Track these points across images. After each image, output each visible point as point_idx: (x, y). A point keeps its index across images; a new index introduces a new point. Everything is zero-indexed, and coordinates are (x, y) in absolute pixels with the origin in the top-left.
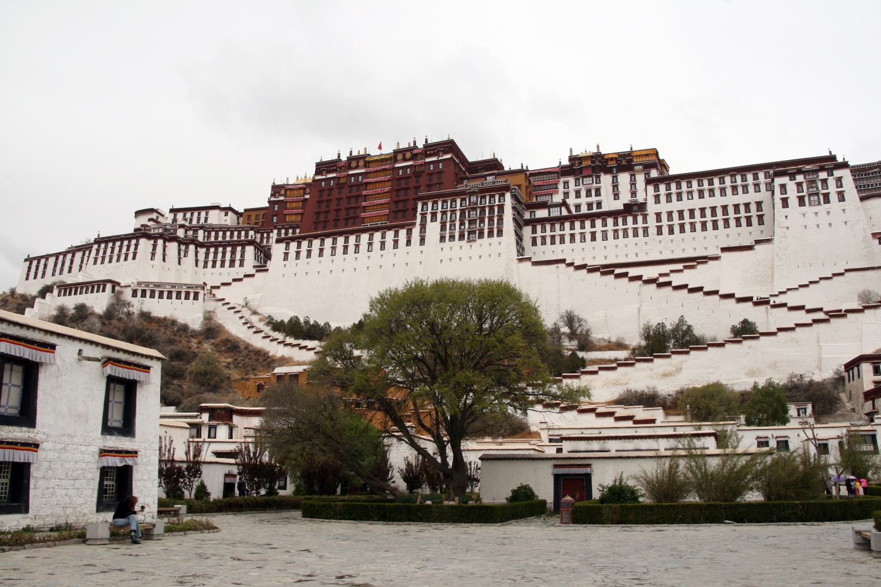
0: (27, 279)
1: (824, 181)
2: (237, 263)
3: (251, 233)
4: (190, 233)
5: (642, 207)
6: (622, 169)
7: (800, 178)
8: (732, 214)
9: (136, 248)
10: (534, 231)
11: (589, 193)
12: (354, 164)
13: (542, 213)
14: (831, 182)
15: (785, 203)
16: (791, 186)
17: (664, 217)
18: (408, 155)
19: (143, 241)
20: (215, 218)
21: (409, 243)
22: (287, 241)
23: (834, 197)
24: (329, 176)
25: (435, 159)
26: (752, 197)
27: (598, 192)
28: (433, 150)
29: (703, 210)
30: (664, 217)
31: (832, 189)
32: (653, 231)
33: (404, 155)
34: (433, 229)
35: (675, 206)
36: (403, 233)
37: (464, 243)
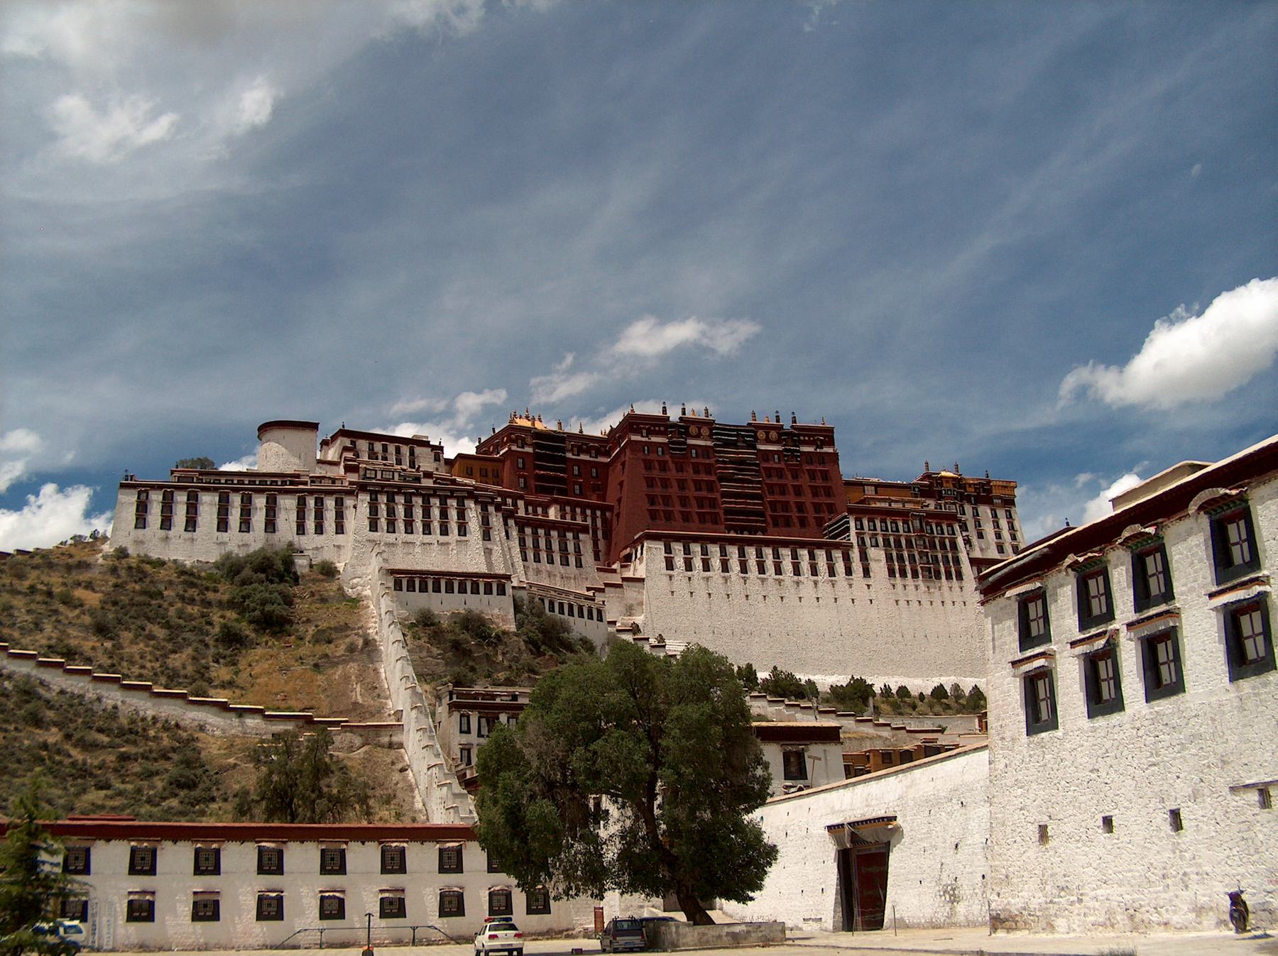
0: (141, 522)
2: (572, 560)
3: (521, 503)
9: (461, 514)
12: (693, 430)
18: (773, 435)
19: (470, 504)
20: (426, 463)
21: (849, 571)
22: (667, 540)
24: (654, 439)
25: (811, 449)
28: (809, 436)
33: (767, 434)
34: (877, 556)
36: (837, 554)
37: (920, 581)
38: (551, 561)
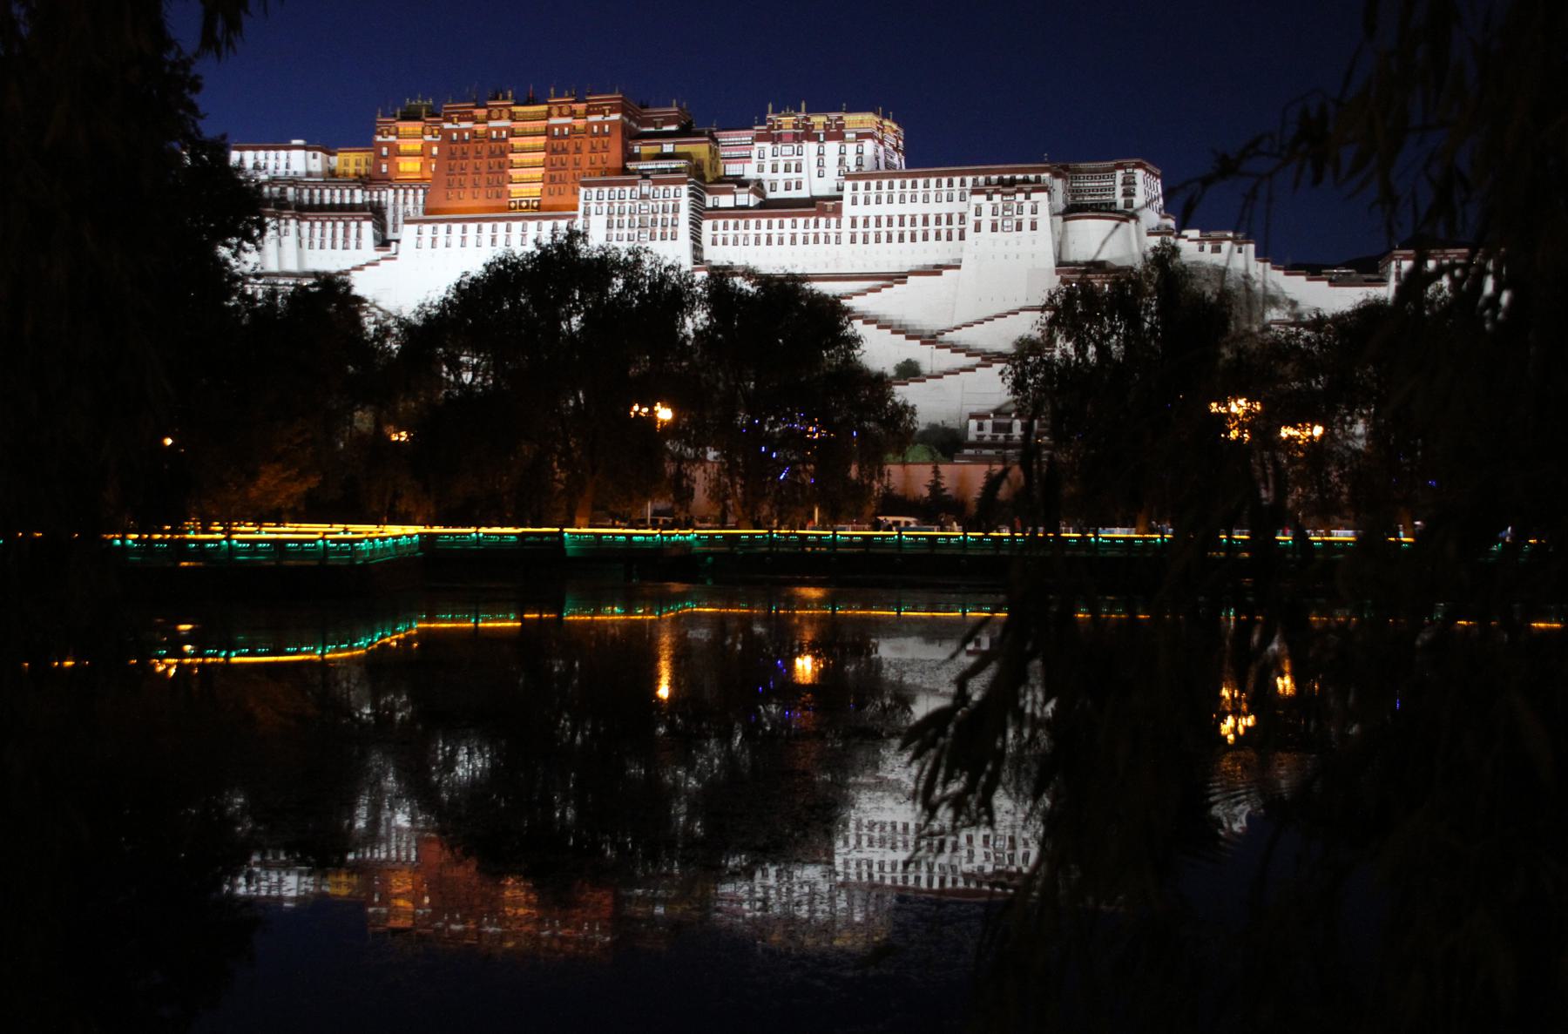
1: (1020, 204)
2: (353, 242)
3: (358, 192)
4: (276, 190)
5: (837, 211)
6: (829, 137)
7: (997, 198)
8: (932, 227)
10: (715, 228)
11: (787, 170)
12: (495, 113)
13: (726, 201)
14: (1027, 205)
15: (978, 228)
16: (987, 207)
17: (860, 222)
18: (566, 111)
23: (1026, 225)
25: (599, 118)
26: (956, 207)
27: (798, 170)
29: (902, 218)
30: (860, 222)
31: (1027, 218)
32: (846, 237)
35: (873, 210)
38: (333, 247)
